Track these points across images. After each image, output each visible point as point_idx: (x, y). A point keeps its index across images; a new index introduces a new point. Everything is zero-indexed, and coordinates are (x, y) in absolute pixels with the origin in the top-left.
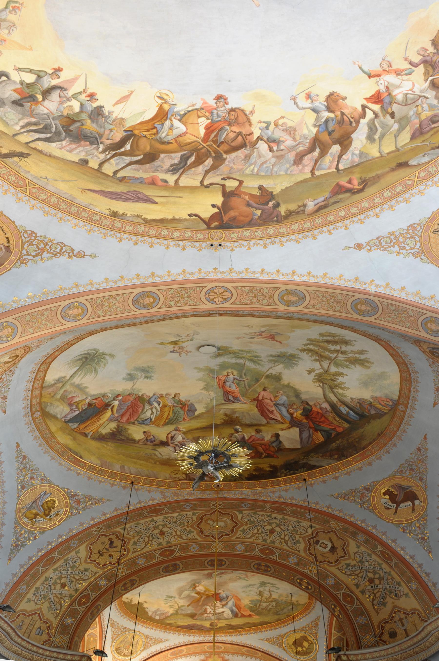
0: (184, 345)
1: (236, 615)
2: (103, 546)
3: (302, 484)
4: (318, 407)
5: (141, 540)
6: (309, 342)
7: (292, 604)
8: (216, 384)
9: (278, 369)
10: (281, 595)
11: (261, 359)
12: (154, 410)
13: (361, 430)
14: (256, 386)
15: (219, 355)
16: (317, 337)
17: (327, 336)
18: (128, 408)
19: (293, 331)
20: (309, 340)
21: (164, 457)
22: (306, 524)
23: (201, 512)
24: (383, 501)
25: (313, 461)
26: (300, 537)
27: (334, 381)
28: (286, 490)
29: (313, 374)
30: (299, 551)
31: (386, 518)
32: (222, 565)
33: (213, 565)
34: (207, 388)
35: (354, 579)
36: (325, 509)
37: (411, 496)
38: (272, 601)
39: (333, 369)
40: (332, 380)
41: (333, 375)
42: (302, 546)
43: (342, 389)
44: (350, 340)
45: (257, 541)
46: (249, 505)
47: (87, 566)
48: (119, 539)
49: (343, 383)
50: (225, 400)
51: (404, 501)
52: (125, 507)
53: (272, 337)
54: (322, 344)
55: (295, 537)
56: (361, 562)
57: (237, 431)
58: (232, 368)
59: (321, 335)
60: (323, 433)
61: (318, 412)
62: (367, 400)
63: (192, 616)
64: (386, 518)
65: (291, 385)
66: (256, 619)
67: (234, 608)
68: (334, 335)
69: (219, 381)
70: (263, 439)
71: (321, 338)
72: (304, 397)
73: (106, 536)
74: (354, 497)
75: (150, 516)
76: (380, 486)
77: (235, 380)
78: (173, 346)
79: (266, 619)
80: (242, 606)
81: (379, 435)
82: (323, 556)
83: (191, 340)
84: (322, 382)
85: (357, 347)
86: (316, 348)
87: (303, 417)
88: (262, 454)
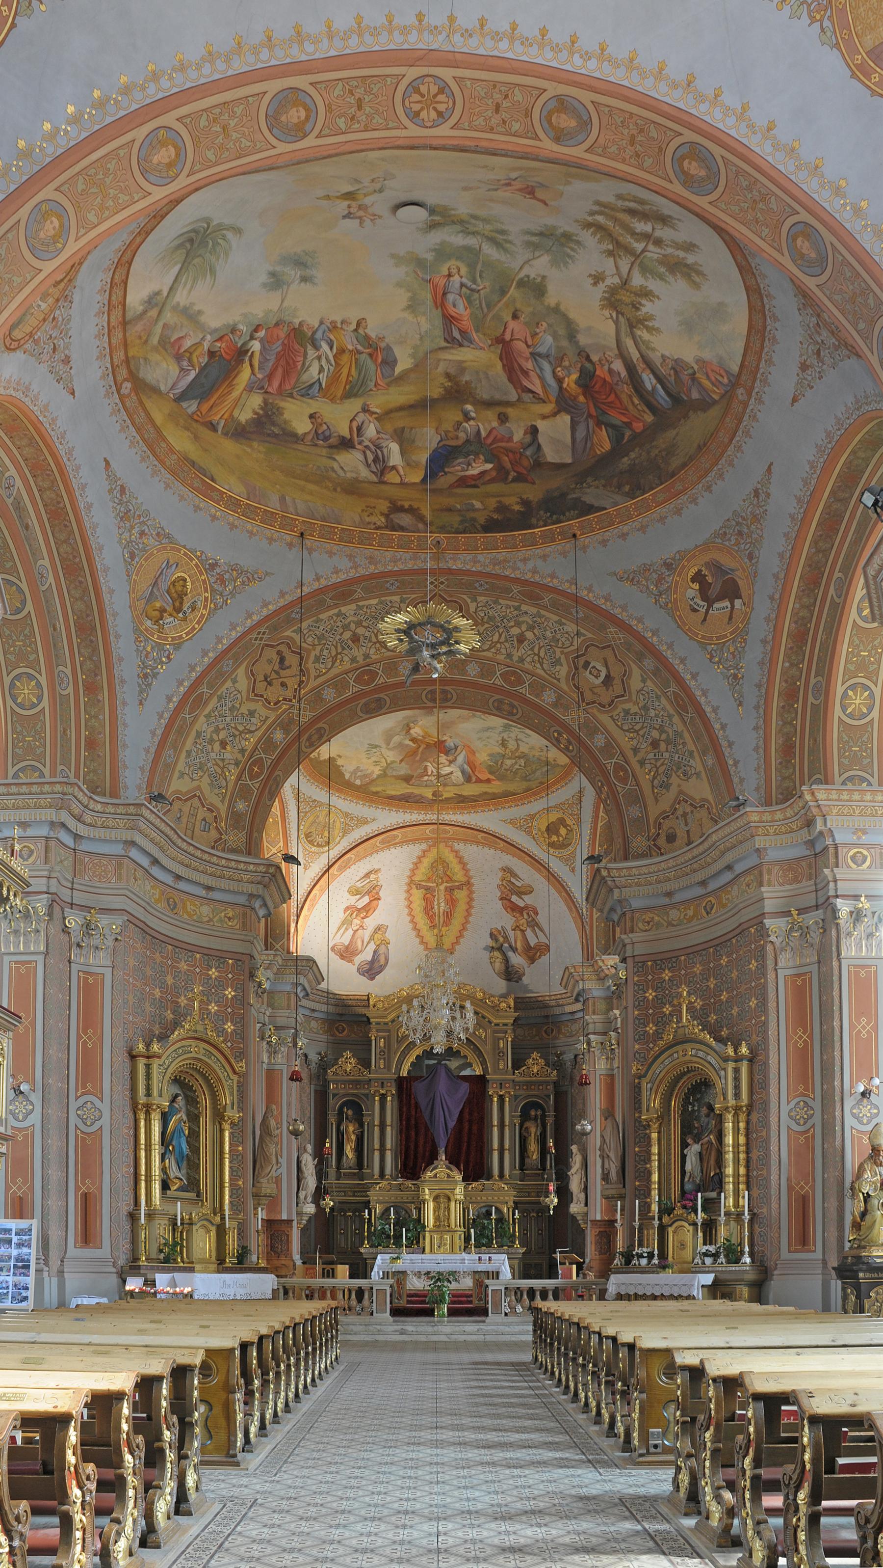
0: (368, 201)
1: (468, 779)
2: (270, 668)
3: (569, 546)
4: (606, 367)
5: (325, 652)
6: (596, 208)
7: (547, 763)
8: (429, 296)
9: (540, 266)
10: (532, 748)
11: (510, 238)
12: (324, 362)
13: (671, 433)
14: (500, 305)
15: (433, 226)
16: (611, 199)
17: (629, 201)
18: (278, 358)
19: (570, 183)
20: (598, 203)
21: (349, 475)
22: (571, 628)
23: (413, 596)
24: (690, 593)
25: (590, 495)
26: (562, 653)
27: (638, 309)
28: (544, 557)
29: (602, 286)
30: (558, 680)
31: (690, 630)
32: (447, 700)
33: (434, 700)
34: (413, 307)
35: (632, 738)
36: (601, 602)
37: (731, 591)
38: (519, 757)
39: (637, 280)
40: (634, 306)
41: (636, 294)
42: (563, 671)
43: (649, 329)
44: (670, 217)
45: (498, 657)
46: (487, 586)
47: (252, 706)
48: (293, 652)
49: (651, 318)
50: (446, 340)
51: (720, 598)
52: (296, 588)
53: (530, 191)
54: (621, 216)
55: (554, 652)
56: (645, 708)
57: (467, 417)
58: (458, 258)
59: (619, 197)
60: (610, 430)
61: (605, 380)
62: (688, 366)
63: (407, 779)
64: (690, 630)
65: (562, 308)
66: (496, 787)
67: (466, 766)
68: (642, 202)
69: (435, 287)
70: (510, 439)
71: (620, 203)
72: (583, 340)
73: (272, 646)
74: (647, 581)
75: (336, 606)
76: (688, 561)
77: (464, 289)
78: (347, 203)
79: (511, 787)
80: (477, 764)
81: (699, 448)
82: (594, 693)
83: (381, 191)
84: (615, 308)
85: (682, 236)
86: (610, 224)
87: (579, 390)
88: (508, 473)
